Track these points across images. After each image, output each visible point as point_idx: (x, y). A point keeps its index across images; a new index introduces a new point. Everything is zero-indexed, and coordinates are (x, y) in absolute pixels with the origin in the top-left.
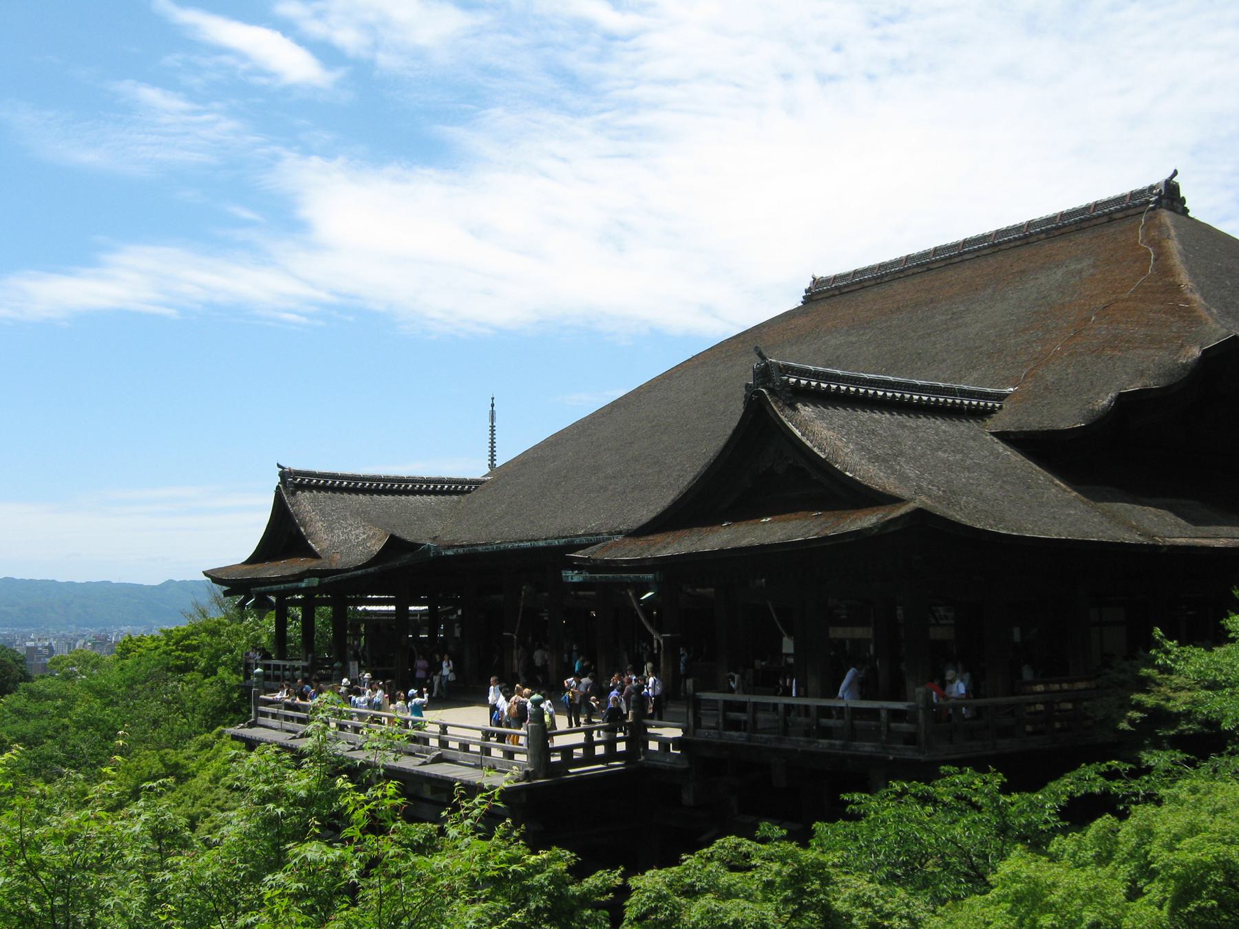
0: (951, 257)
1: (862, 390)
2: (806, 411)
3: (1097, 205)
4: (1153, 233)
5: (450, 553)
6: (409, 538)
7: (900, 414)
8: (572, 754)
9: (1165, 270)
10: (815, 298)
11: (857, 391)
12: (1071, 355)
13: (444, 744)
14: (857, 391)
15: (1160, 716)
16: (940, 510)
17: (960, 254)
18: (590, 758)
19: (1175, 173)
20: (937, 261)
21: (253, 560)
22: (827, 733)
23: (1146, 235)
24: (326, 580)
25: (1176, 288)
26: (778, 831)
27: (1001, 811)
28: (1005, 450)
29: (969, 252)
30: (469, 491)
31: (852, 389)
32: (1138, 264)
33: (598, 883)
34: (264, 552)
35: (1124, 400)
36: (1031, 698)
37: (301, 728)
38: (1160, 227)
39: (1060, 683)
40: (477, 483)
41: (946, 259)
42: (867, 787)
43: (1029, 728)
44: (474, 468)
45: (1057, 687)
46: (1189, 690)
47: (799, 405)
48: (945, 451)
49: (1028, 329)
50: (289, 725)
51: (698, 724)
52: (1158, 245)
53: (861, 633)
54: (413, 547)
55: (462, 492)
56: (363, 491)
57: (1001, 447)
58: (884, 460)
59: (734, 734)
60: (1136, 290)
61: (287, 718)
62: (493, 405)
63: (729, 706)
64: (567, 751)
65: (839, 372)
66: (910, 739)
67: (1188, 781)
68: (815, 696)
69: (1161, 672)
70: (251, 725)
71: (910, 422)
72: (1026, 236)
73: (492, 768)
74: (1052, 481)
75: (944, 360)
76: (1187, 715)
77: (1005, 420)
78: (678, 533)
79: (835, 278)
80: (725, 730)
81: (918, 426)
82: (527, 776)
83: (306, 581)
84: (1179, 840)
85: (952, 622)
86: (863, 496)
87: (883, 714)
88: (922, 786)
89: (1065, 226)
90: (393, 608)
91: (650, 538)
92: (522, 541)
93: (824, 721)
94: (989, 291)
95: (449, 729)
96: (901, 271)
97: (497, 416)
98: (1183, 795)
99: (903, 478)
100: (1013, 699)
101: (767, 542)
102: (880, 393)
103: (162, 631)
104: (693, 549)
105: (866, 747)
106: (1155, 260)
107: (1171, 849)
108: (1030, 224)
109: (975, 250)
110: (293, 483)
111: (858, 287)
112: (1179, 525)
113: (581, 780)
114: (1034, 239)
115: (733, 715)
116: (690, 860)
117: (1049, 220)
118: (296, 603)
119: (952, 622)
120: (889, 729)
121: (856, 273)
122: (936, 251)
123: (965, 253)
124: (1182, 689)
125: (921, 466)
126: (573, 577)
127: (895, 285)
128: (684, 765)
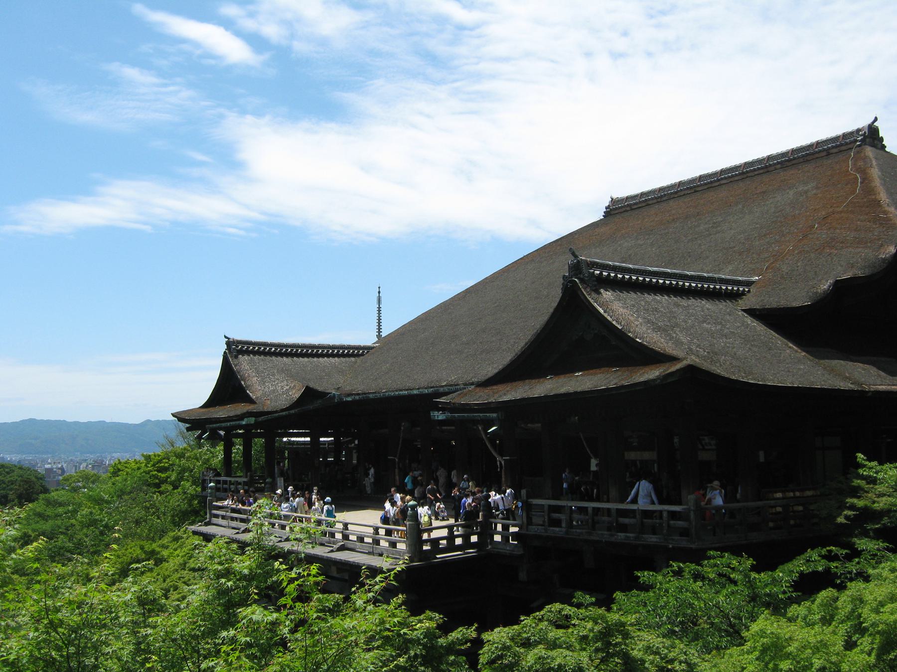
0: (711, 182)
1: (647, 280)
2: (607, 295)
3: (818, 143)
4: (860, 163)
5: (349, 399)
6: (320, 389)
7: (675, 296)
8: (439, 544)
9: (869, 190)
10: (613, 212)
11: (644, 280)
12: (801, 252)
13: (346, 537)
14: (644, 280)
15: (868, 515)
16: (706, 366)
17: (718, 180)
18: (451, 547)
19: (876, 119)
20: (701, 185)
21: (210, 404)
22: (623, 528)
23: (854, 165)
24: (260, 419)
25: (877, 203)
26: (589, 599)
27: (751, 584)
28: (752, 322)
29: (725, 178)
30: (362, 355)
31: (641, 279)
32: (849, 186)
33: (459, 636)
34: (215, 400)
35: (839, 285)
36: (772, 502)
37: (243, 526)
38: (865, 158)
39: (793, 491)
40: (368, 348)
41: (708, 183)
42: (654, 568)
43: (771, 524)
44: (368, 338)
45: (791, 494)
46: (889, 496)
47: (602, 291)
48: (709, 323)
49: (768, 234)
50: (234, 524)
51: (530, 522)
52: (864, 172)
53: (647, 455)
54: (323, 395)
55: (358, 355)
56: (286, 355)
57: (749, 320)
58: (665, 330)
59: (557, 529)
60: (848, 205)
62: (379, 292)
64: (435, 542)
65: (631, 266)
66: (685, 533)
67: (889, 563)
68: (615, 502)
69: (868, 483)
70: (207, 524)
71: (684, 302)
72: (766, 167)
73: (381, 555)
74: (787, 345)
75: (707, 257)
76: (887, 512)
77: (752, 300)
78: (515, 384)
79: (627, 198)
80: (550, 526)
81: (689, 306)
83: (246, 420)
84: (883, 606)
85: (714, 447)
86: (649, 356)
87: (665, 515)
88: (693, 566)
89: (794, 159)
90: (308, 439)
91: (495, 387)
92: (401, 390)
93: (621, 520)
94: (740, 206)
95: (349, 526)
96: (676, 193)
97: (383, 300)
98: (885, 573)
99: (678, 343)
100: (760, 503)
101: (579, 389)
102: (661, 281)
103: (143, 455)
104: (525, 395)
105: (653, 539)
106: (861, 183)
107: (877, 611)
108: (770, 158)
109: (729, 177)
110: (236, 349)
111: (644, 204)
112: (880, 376)
113: (445, 563)
114: (772, 168)
115: (556, 515)
116: (527, 621)
117: (783, 155)
118: (238, 436)
119: (714, 447)
120: (669, 526)
121: (642, 194)
122: (701, 178)
123: (722, 179)
124: (883, 495)
125: (691, 334)
126: (439, 416)
127: (671, 203)
128: (520, 552)
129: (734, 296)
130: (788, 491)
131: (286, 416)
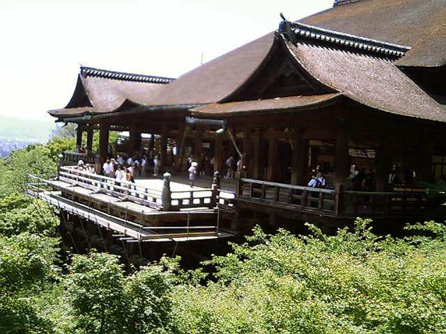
2: (303, 47)
18: (191, 205)
21: (67, 107)
30: (168, 83)
37: (75, 182)
47: (298, 44)
51: (241, 193)
54: (138, 105)
55: (165, 83)
56: (118, 78)
61: (70, 178)
63: (255, 185)
64: (180, 201)
73: (148, 206)
82: (161, 210)
87: (321, 194)
110: (86, 73)
129: (393, 57)
130: (408, 187)
131: (112, 117)
